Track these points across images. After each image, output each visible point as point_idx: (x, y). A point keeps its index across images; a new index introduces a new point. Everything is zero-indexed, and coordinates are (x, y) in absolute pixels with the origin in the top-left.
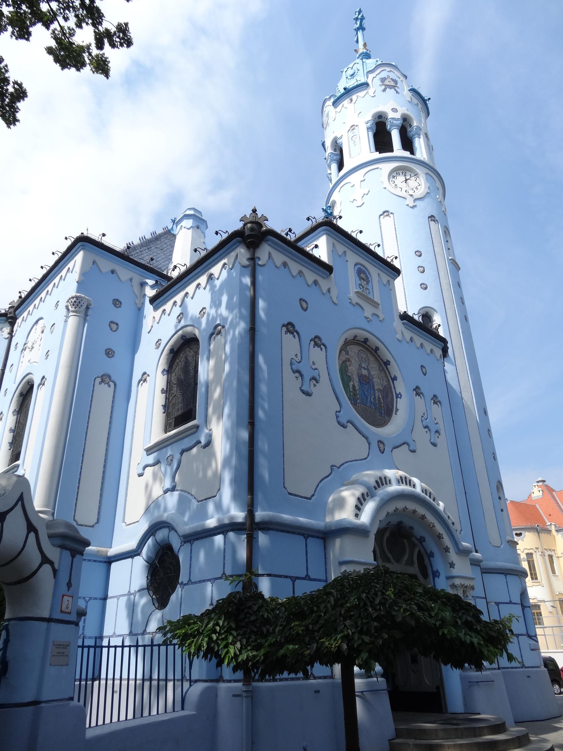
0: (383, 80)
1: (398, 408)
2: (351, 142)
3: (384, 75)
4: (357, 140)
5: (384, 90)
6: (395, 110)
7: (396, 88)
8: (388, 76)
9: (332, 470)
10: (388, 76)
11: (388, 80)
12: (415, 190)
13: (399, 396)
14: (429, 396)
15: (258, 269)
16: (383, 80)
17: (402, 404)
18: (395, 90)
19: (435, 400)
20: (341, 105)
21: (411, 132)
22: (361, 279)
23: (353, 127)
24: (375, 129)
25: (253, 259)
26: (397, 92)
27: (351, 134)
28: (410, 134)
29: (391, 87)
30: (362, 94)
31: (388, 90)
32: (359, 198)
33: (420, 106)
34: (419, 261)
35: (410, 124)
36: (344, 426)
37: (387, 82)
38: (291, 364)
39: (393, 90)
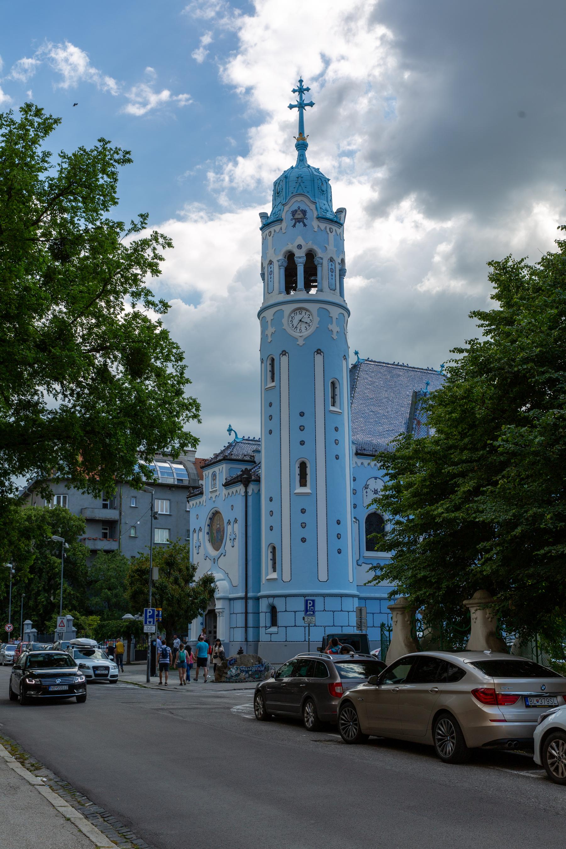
0: (294, 213)
3: (295, 207)
4: (272, 276)
5: (294, 226)
7: (305, 221)
8: (299, 208)
10: (299, 208)
11: (299, 212)
12: (307, 327)
16: (294, 213)
18: (303, 223)
23: (271, 262)
24: (285, 264)
26: (305, 225)
28: (316, 263)
30: (277, 228)
31: (297, 223)
33: (328, 226)
39: (301, 223)
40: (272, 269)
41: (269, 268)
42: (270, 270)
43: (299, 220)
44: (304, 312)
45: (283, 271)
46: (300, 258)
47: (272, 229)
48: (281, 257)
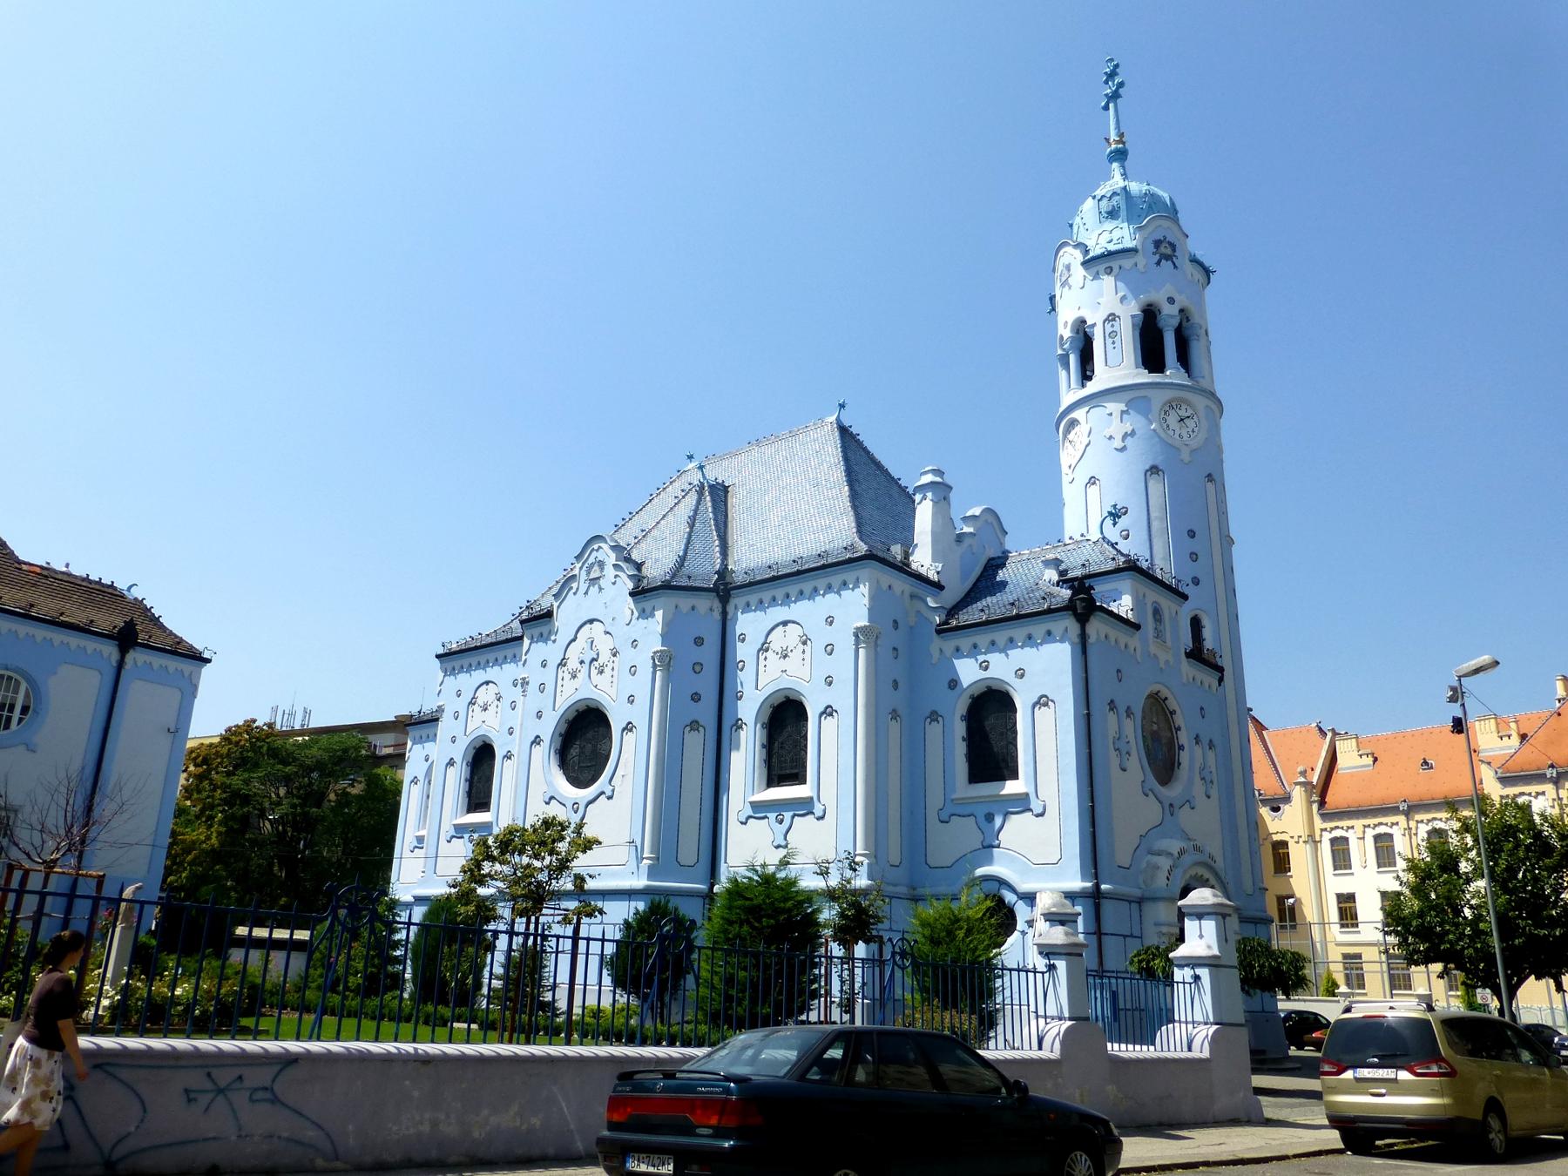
0: (1157, 244)
2: (1109, 341)
4: (1117, 339)
5: (1158, 263)
6: (1171, 300)
13: (1181, 748)
14: (1205, 741)
16: (1157, 244)
17: (1184, 757)
19: (1211, 745)
21: (1186, 333)
23: (1112, 318)
27: (1108, 326)
29: (1168, 258)
32: (1118, 437)
34: (1193, 545)
37: (1162, 250)
41: (1108, 326)
42: (1109, 329)
47: (1115, 265)
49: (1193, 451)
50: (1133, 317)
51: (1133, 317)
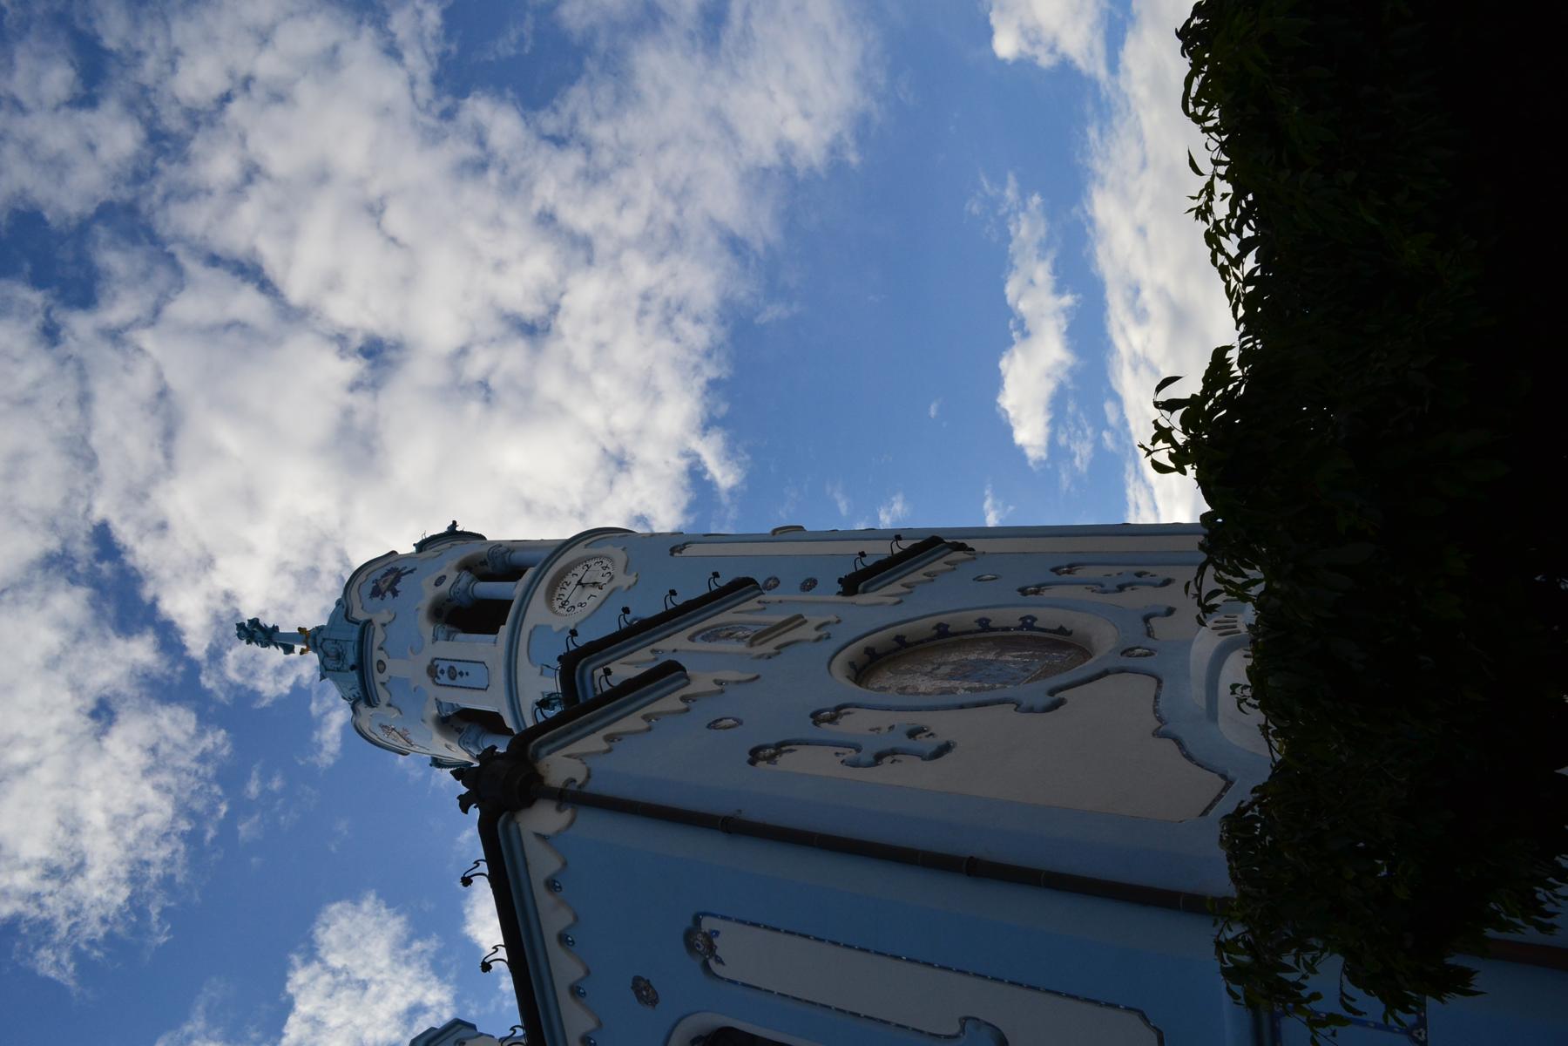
0: (376, 592)
1: (1056, 627)
2: (459, 681)
4: (459, 667)
5: (395, 593)
6: (439, 581)
9: (1164, 735)
10: (376, 581)
15: (592, 788)
16: (376, 592)
20: (379, 688)
22: (728, 636)
23: (432, 671)
25: (567, 797)
30: (378, 637)
31: (397, 587)
35: (484, 563)
36: (1060, 703)
37: (384, 586)
38: (855, 764)
40: (444, 666)
42: (444, 679)
43: (397, 580)
44: (567, 579)
45: (461, 636)
46: (458, 581)
47: (378, 655)
48: (427, 629)
49: (626, 570)
50: (436, 639)
51: (436, 639)
